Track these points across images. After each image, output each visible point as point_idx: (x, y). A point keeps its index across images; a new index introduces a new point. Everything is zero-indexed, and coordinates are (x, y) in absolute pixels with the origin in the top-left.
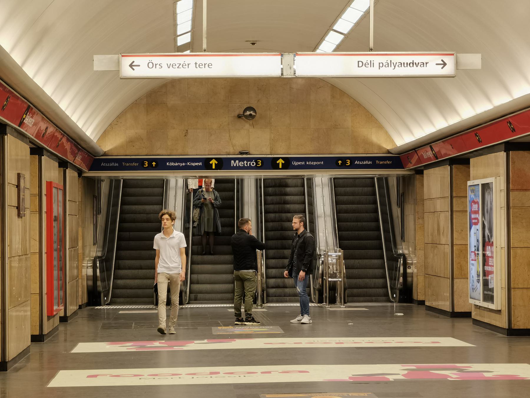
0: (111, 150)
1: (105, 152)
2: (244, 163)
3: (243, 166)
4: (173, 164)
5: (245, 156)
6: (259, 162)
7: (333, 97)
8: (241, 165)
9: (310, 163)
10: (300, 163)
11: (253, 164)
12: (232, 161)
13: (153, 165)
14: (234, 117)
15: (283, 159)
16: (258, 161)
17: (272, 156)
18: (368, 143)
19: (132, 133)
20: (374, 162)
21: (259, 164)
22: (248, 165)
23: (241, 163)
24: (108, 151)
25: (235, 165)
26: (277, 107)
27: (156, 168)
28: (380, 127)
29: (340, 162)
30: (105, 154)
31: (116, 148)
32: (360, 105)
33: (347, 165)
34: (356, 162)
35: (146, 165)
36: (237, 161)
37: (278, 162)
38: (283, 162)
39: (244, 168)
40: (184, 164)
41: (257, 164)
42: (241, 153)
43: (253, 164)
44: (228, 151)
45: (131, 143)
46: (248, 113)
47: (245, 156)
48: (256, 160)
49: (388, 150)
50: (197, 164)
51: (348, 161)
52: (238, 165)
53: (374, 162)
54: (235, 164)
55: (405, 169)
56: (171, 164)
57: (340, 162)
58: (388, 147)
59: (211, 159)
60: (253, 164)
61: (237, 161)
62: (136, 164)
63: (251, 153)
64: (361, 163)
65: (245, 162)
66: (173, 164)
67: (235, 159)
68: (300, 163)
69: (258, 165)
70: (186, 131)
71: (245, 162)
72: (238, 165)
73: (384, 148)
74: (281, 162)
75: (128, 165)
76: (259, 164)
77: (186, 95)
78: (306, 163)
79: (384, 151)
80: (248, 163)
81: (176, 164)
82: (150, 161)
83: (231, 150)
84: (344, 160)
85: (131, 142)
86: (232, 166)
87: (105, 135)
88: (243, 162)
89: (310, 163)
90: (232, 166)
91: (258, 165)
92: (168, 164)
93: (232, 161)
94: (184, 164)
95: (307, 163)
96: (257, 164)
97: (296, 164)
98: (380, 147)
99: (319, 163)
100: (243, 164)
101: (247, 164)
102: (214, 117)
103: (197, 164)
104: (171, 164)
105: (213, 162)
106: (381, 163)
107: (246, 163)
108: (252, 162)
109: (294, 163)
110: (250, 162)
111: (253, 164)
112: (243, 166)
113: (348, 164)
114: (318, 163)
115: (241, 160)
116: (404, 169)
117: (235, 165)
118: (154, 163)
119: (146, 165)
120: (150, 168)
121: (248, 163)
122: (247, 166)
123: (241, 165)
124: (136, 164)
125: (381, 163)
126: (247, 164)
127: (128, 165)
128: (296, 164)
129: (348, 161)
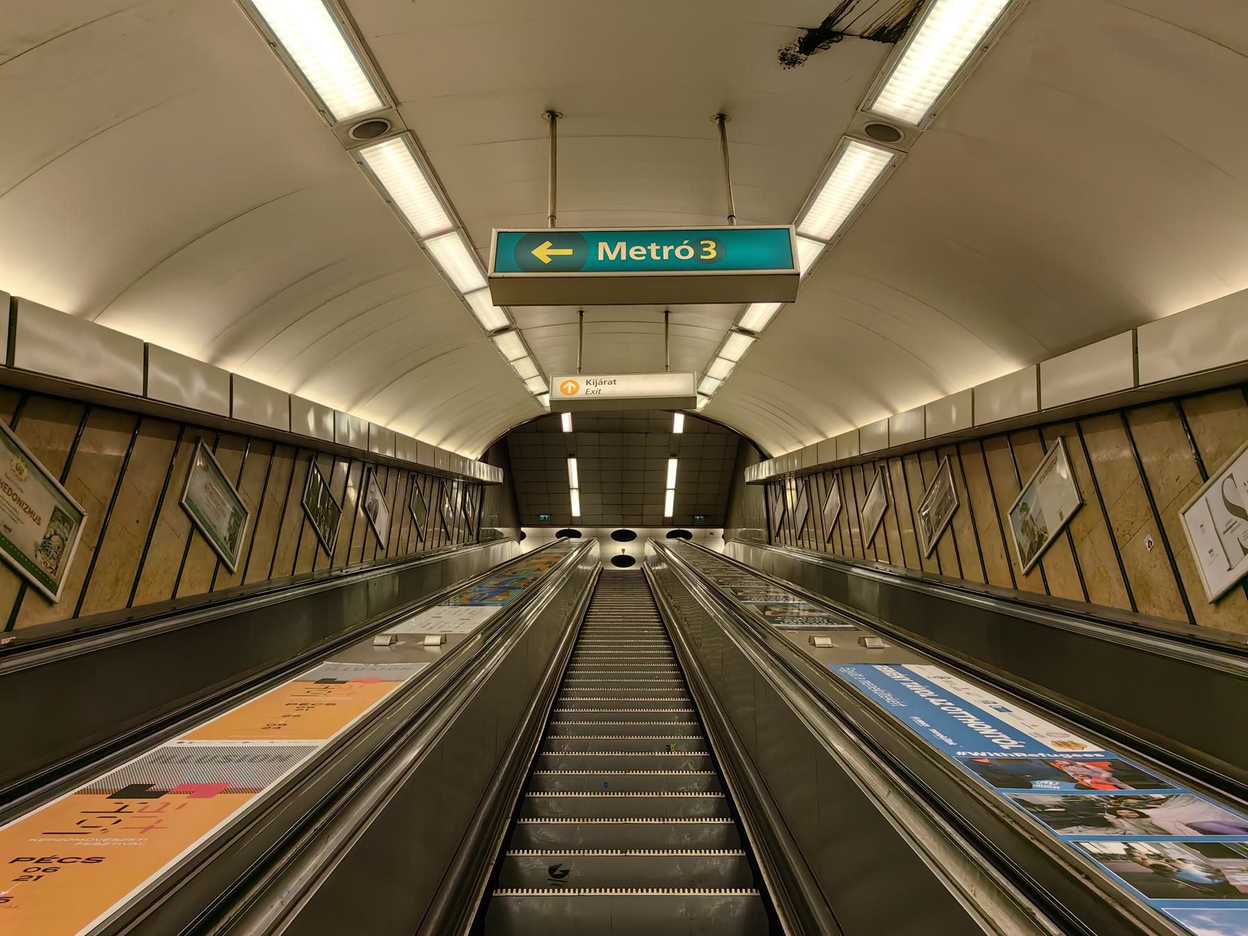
2: (649, 251)
3: (644, 258)
6: (708, 246)
8: (636, 255)
22: (666, 256)
25: (612, 257)
52: (623, 257)
60: (684, 252)
72: (623, 257)
80: (666, 250)
86: (601, 257)
88: (646, 248)
90: (601, 257)
100: (644, 251)
101: (659, 252)
107: (657, 250)
110: (672, 247)
112: (644, 258)
121: (666, 250)
122: (659, 258)
123: (636, 255)
126: (659, 252)
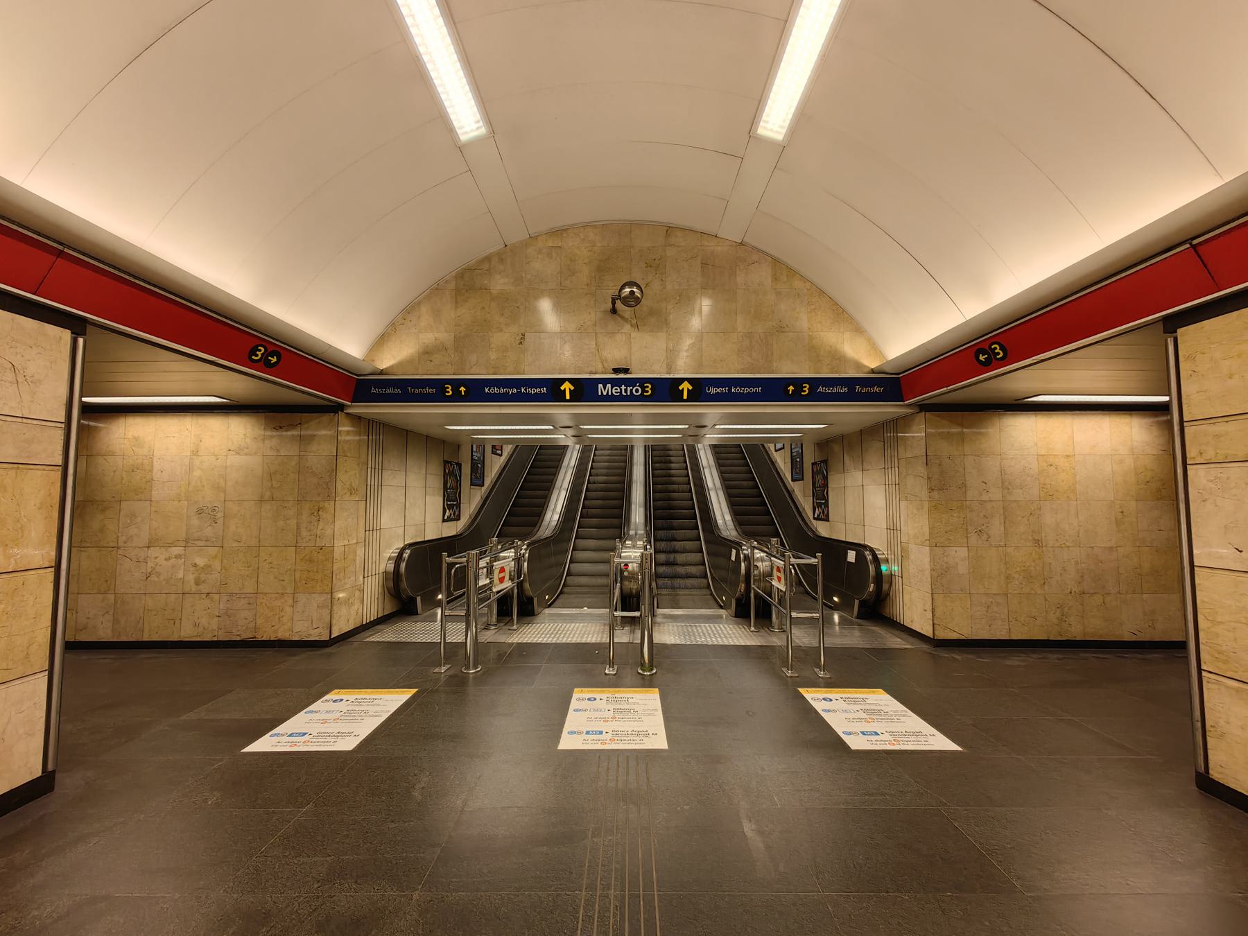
0: (392, 367)
1: (382, 370)
2: (621, 390)
4: (496, 390)
5: (622, 376)
6: (647, 387)
7: (775, 279)
8: (616, 392)
9: (738, 390)
10: (719, 390)
11: (637, 390)
12: (600, 386)
13: (461, 391)
14: (605, 311)
15: (690, 380)
16: (645, 385)
17: (671, 376)
18: (838, 358)
19: (429, 338)
20: (852, 389)
21: (647, 392)
22: (629, 394)
23: (616, 389)
24: (386, 368)
25: (605, 393)
26: (679, 296)
27: (468, 398)
28: (858, 330)
29: (791, 388)
30: (382, 372)
31: (400, 364)
32: (822, 293)
33: (802, 393)
34: (820, 389)
35: (448, 392)
36: (609, 386)
37: (681, 388)
38: (691, 388)
39: (621, 398)
40: (515, 391)
41: (644, 391)
42: (616, 371)
43: (637, 390)
44: (592, 370)
45: (427, 356)
46: (627, 290)
47: (622, 376)
48: (642, 382)
49: (872, 369)
50: (538, 390)
51: (805, 387)
52: (610, 394)
53: (852, 389)
54: (605, 390)
55: (906, 402)
56: (492, 391)
57: (791, 388)
58: (873, 363)
59: (563, 381)
60: (637, 391)
61: (609, 386)
62: (431, 391)
63: (632, 370)
64: (829, 390)
65: (623, 387)
66: (496, 390)
67: (605, 382)
68: (719, 390)
69: (645, 394)
70: (522, 335)
71: (623, 387)
72: (610, 394)
73: (865, 366)
74: (686, 386)
75: (417, 391)
76: (647, 392)
77: (524, 275)
78: (730, 390)
79: (867, 370)
80: (629, 389)
81: (502, 391)
82: (456, 383)
83: (600, 367)
84: (798, 382)
85: (427, 353)
86: (600, 394)
87: (381, 341)
89: (738, 390)
90: (600, 394)
91: (645, 394)
92: (486, 390)
93: (600, 386)
94: (515, 391)
95: (733, 390)
96: (644, 391)
97: (713, 391)
98: (859, 366)
99: (754, 390)
100: (619, 390)
102: (569, 313)
103: (538, 390)
104: (492, 391)
105: (567, 386)
106: (864, 390)
108: (635, 388)
109: (709, 390)
111: (637, 391)
113: (805, 391)
114: (751, 390)
115: (615, 382)
116: (902, 403)
117: (605, 393)
118: (462, 389)
119: (448, 392)
120: (457, 398)
121: (629, 389)
123: (616, 392)
124: (431, 391)
125: (864, 390)
127: (417, 391)
128: (713, 391)
129: (805, 387)
